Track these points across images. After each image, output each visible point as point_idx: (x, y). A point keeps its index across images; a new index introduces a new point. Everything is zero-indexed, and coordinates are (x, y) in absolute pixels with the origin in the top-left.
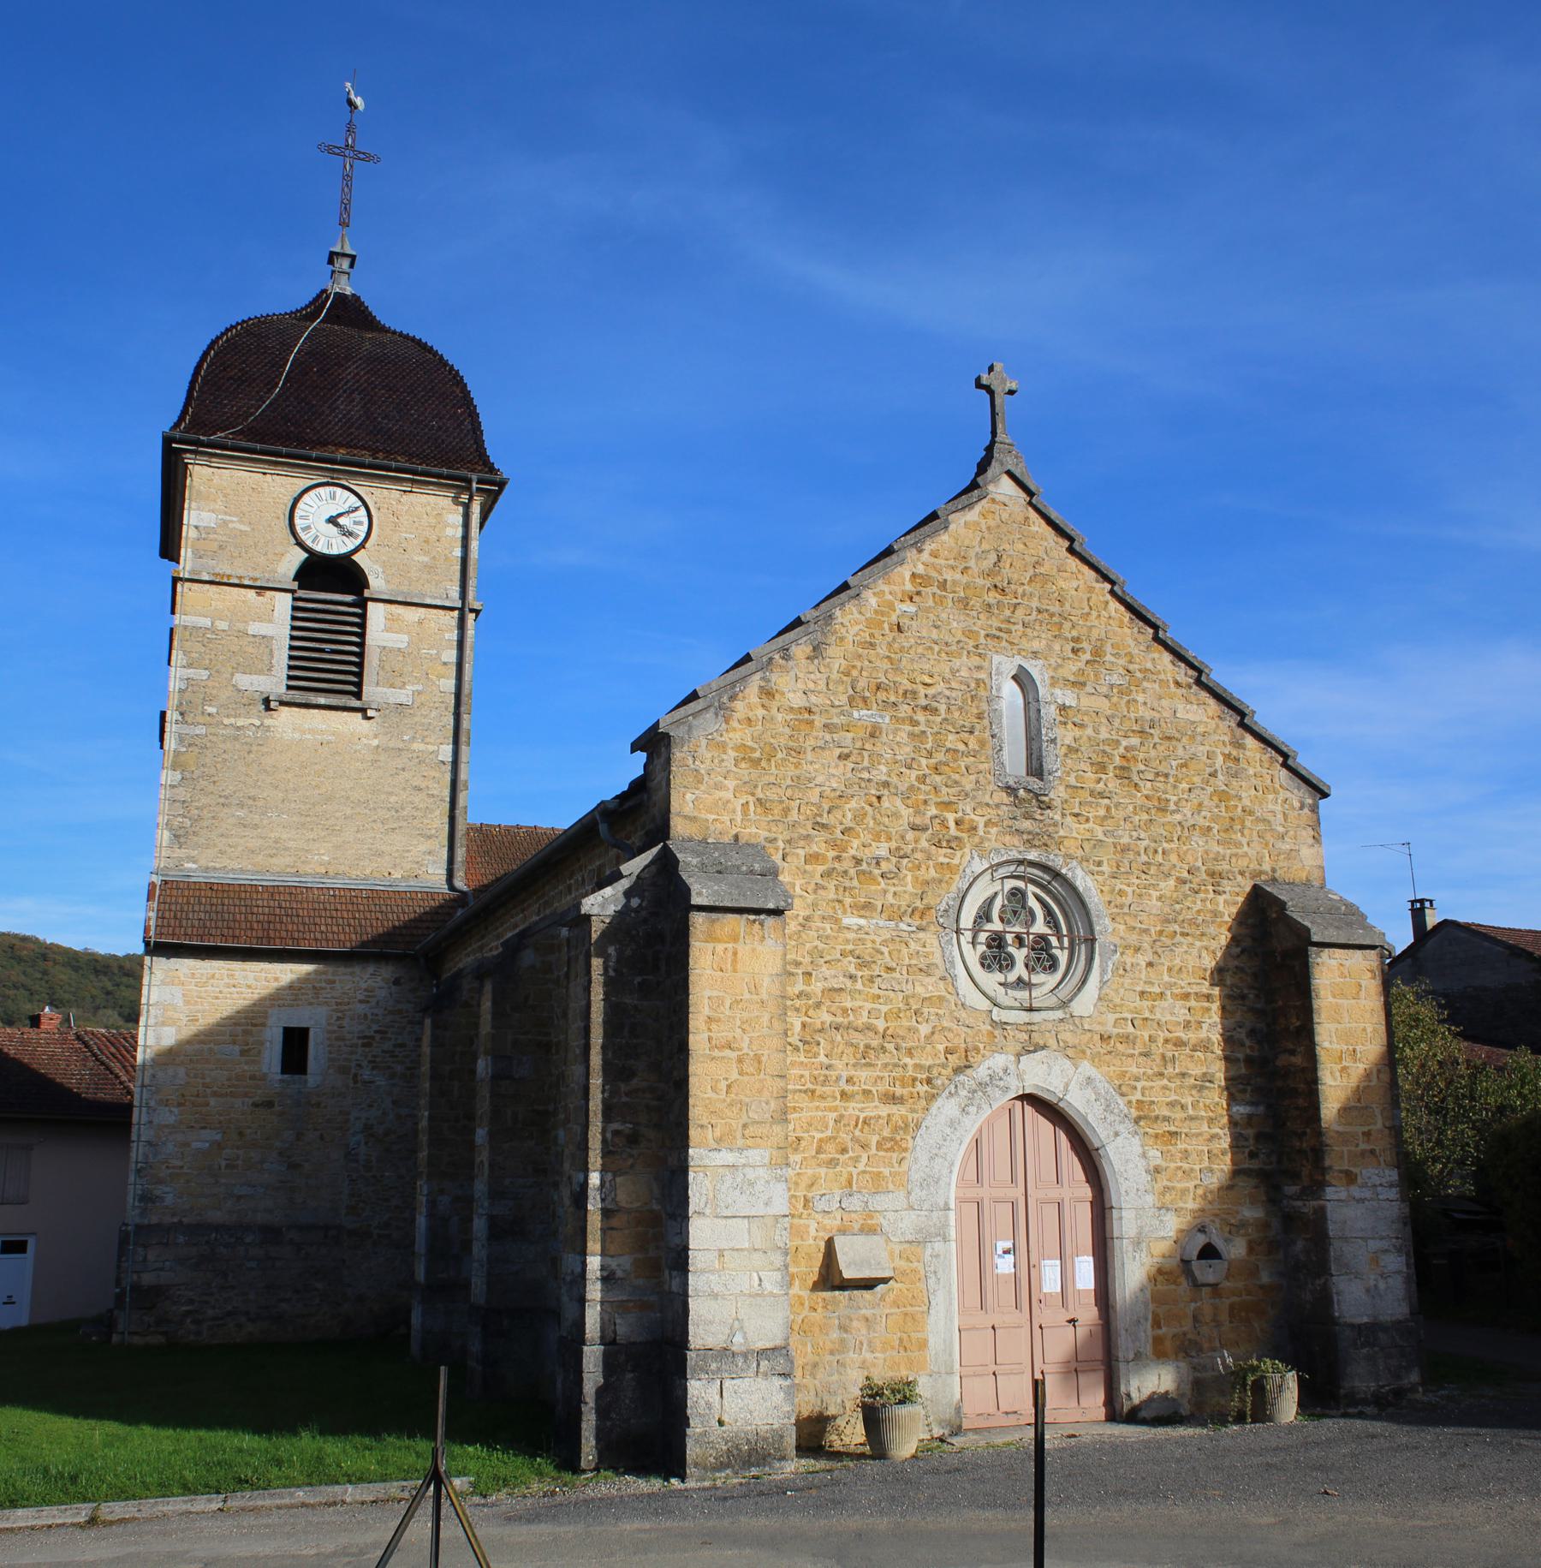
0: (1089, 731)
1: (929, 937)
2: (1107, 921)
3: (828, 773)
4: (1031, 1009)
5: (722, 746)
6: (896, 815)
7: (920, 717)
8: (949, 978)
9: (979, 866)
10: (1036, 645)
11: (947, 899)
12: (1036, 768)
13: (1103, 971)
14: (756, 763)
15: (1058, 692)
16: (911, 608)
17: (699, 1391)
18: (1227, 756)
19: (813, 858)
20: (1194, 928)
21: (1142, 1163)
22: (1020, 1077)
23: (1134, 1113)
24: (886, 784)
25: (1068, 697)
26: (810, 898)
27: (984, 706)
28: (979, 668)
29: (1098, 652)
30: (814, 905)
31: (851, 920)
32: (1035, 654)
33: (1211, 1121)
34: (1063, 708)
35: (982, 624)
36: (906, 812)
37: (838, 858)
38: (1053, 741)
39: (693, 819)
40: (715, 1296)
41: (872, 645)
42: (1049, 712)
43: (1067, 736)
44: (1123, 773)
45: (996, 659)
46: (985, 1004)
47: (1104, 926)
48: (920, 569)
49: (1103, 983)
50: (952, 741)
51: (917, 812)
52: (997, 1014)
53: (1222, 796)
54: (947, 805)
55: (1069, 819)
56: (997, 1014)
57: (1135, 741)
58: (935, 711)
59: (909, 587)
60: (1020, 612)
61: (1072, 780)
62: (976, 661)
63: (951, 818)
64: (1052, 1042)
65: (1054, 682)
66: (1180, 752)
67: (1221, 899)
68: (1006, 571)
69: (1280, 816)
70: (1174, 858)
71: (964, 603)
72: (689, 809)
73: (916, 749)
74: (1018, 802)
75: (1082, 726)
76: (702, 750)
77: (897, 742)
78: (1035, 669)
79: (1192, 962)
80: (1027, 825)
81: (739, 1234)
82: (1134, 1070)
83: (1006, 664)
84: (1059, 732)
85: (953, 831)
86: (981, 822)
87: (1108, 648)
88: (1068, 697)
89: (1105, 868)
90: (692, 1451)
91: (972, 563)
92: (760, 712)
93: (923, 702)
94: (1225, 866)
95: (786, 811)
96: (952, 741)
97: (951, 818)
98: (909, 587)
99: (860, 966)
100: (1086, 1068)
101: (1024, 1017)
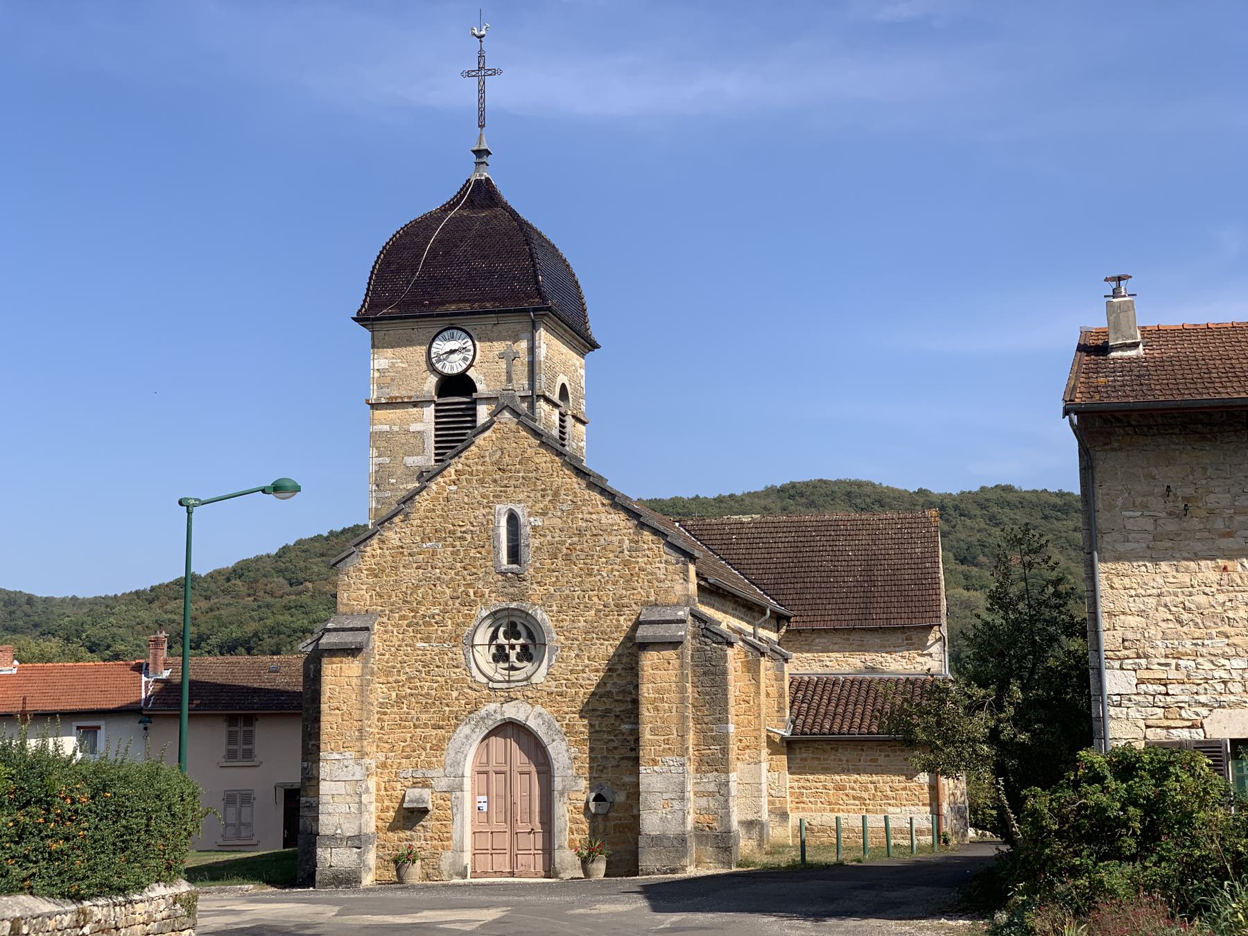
0: (549, 538)
1: (458, 650)
2: (554, 635)
3: (411, 575)
4: (508, 682)
5: (360, 570)
6: (444, 593)
7: (458, 543)
8: (468, 668)
9: (485, 613)
10: (521, 496)
11: (468, 630)
12: (514, 555)
13: (550, 660)
14: (376, 576)
15: (532, 519)
16: (454, 488)
17: (322, 854)
18: (631, 541)
19: (403, 618)
20: (604, 636)
21: (566, 755)
22: (502, 714)
23: (564, 730)
24: (439, 579)
25: (539, 522)
26: (401, 636)
27: (491, 533)
28: (489, 514)
29: (556, 494)
30: (403, 640)
31: (420, 644)
32: (520, 502)
33: (609, 732)
34: (534, 528)
35: (491, 489)
36: (448, 591)
37: (414, 617)
38: (528, 546)
39: (347, 605)
40: (329, 814)
41: (434, 511)
42: (526, 531)
43: (535, 542)
44: (567, 558)
45: (498, 507)
46: (485, 680)
47: (554, 638)
48: (460, 467)
49: (550, 666)
50: (473, 552)
51: (455, 591)
52: (491, 684)
53: (626, 564)
54: (469, 585)
55: (535, 586)
56: (491, 684)
57: (575, 539)
58: (464, 539)
59: (454, 477)
60: (513, 482)
61: (538, 565)
62: (488, 510)
63: (471, 591)
64: (519, 695)
65: (530, 515)
66: (602, 542)
67: (622, 618)
68: (507, 459)
69: (663, 571)
70: (595, 599)
71: (482, 482)
72: (345, 601)
73: (455, 560)
74: (507, 579)
75: (544, 536)
76: (351, 573)
77: (445, 553)
78: (519, 510)
79: (602, 652)
80: (511, 590)
81: (340, 788)
82: (566, 709)
83: (502, 509)
84: (531, 540)
85: (472, 597)
86: (487, 591)
87: (563, 492)
88: (539, 522)
89: (555, 608)
90: (318, 878)
91: (487, 459)
92: (379, 551)
93: (459, 535)
94: (626, 601)
95: (390, 597)
96: (473, 552)
97: (471, 591)
98: (454, 477)
99: (424, 667)
100: (538, 708)
101: (505, 685)
